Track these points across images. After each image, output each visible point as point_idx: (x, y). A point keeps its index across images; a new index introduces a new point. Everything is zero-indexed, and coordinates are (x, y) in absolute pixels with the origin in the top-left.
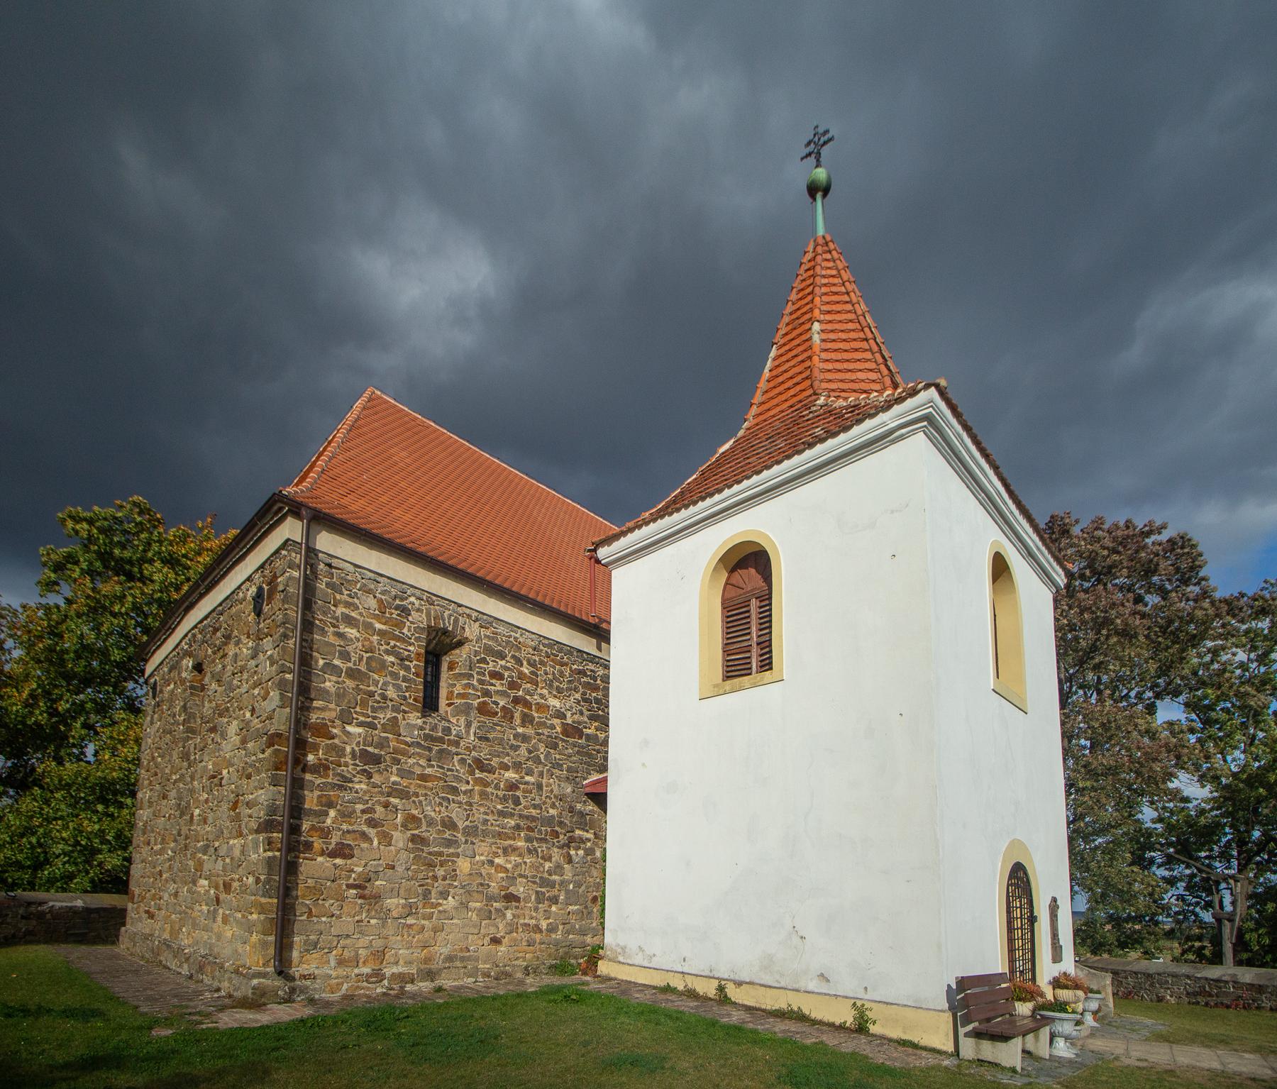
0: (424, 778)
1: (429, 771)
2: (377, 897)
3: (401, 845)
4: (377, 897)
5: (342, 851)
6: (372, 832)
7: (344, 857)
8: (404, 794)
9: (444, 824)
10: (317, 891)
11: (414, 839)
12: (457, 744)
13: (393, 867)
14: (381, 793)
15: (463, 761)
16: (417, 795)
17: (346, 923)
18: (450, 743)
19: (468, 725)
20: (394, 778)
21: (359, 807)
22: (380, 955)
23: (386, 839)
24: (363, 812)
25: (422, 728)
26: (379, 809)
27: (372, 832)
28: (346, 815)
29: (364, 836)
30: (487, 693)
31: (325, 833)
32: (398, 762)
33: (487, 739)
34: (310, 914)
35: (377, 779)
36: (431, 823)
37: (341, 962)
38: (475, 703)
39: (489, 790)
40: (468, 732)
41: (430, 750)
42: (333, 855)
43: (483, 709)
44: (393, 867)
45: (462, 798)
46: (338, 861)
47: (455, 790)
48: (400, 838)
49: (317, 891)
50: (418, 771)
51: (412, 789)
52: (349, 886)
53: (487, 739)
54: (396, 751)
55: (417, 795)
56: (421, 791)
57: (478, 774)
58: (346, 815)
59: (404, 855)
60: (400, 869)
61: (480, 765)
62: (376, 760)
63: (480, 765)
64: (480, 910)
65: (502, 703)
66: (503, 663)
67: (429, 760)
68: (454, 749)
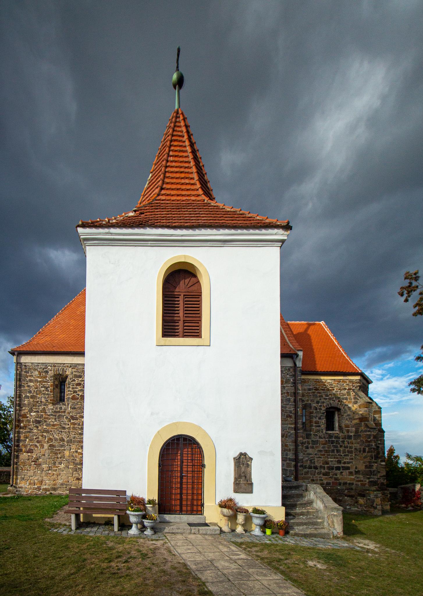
0: (53, 425)
1: (55, 423)
2: (40, 465)
3: (46, 448)
4: (40, 465)
5: (30, 451)
6: (38, 444)
7: (31, 453)
8: (47, 432)
9: (60, 440)
10: (24, 464)
11: (50, 446)
12: (64, 412)
13: (44, 455)
14: (41, 432)
15: (67, 418)
16: (51, 431)
17: (31, 473)
18: (62, 412)
19: (68, 404)
20: (45, 427)
21: (35, 437)
22: (41, 482)
23: (42, 446)
24: (36, 438)
25: (53, 409)
26: (40, 437)
27: (38, 444)
28: (31, 440)
29: (36, 446)
30: (75, 392)
31: (25, 446)
32: (46, 421)
33: (75, 408)
34: (22, 470)
35: (40, 428)
36: (56, 440)
37: (30, 484)
38: (71, 396)
39: (76, 426)
40: (68, 407)
41: (55, 416)
42: (28, 452)
43: (74, 398)
44: (44, 455)
45: (67, 430)
46: (29, 454)
47: (64, 428)
48: (46, 446)
49: (24, 464)
50: (52, 423)
51: (50, 429)
52: (32, 461)
53: (75, 408)
54: (45, 418)
55: (51, 431)
56: (53, 430)
57: (72, 421)
58: (31, 440)
59: (47, 451)
60: (46, 455)
61: (73, 418)
62: (39, 422)
63: (73, 418)
64: (73, 468)
65: (80, 394)
66: (81, 379)
67: (55, 419)
68: (63, 414)
